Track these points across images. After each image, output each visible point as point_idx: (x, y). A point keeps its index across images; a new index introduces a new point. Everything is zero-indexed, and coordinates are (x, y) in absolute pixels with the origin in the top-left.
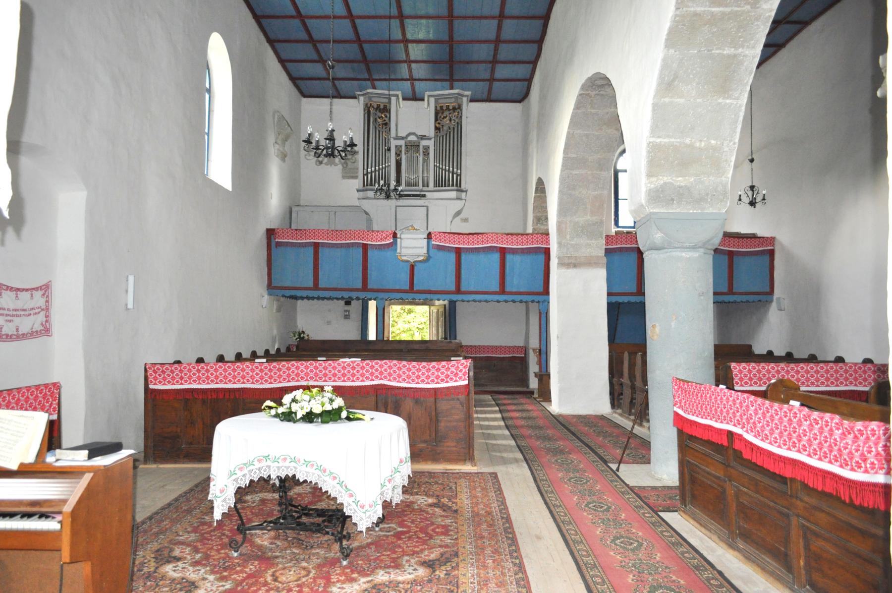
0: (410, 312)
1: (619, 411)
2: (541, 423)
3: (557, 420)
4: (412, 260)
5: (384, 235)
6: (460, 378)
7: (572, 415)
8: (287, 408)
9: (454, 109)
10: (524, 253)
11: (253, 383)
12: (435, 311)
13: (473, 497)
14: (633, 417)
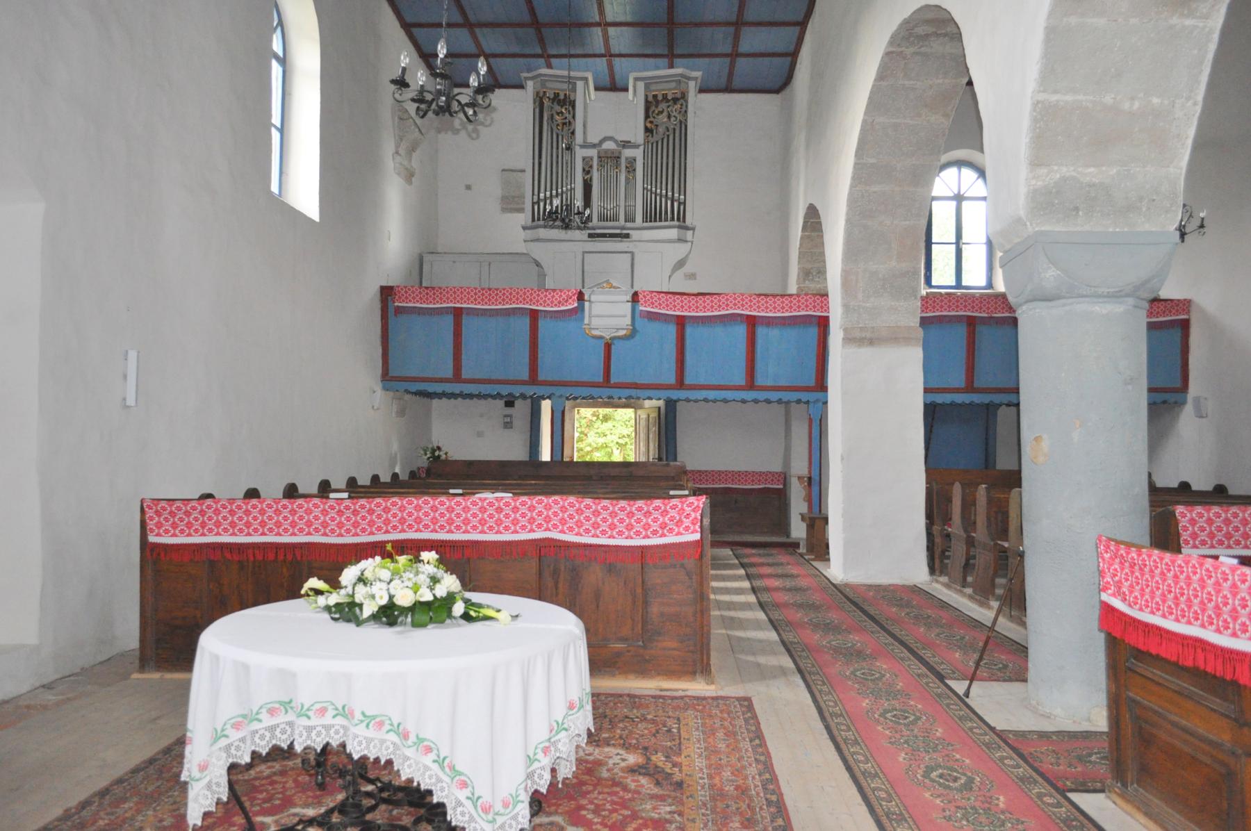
0: (606, 419)
1: (944, 579)
2: (816, 598)
3: (841, 592)
4: (607, 335)
5: (564, 296)
6: (687, 529)
7: (865, 585)
8: (348, 595)
9: (675, 100)
10: (784, 324)
11: (325, 534)
12: (644, 416)
13: (712, 751)
14: (969, 591)
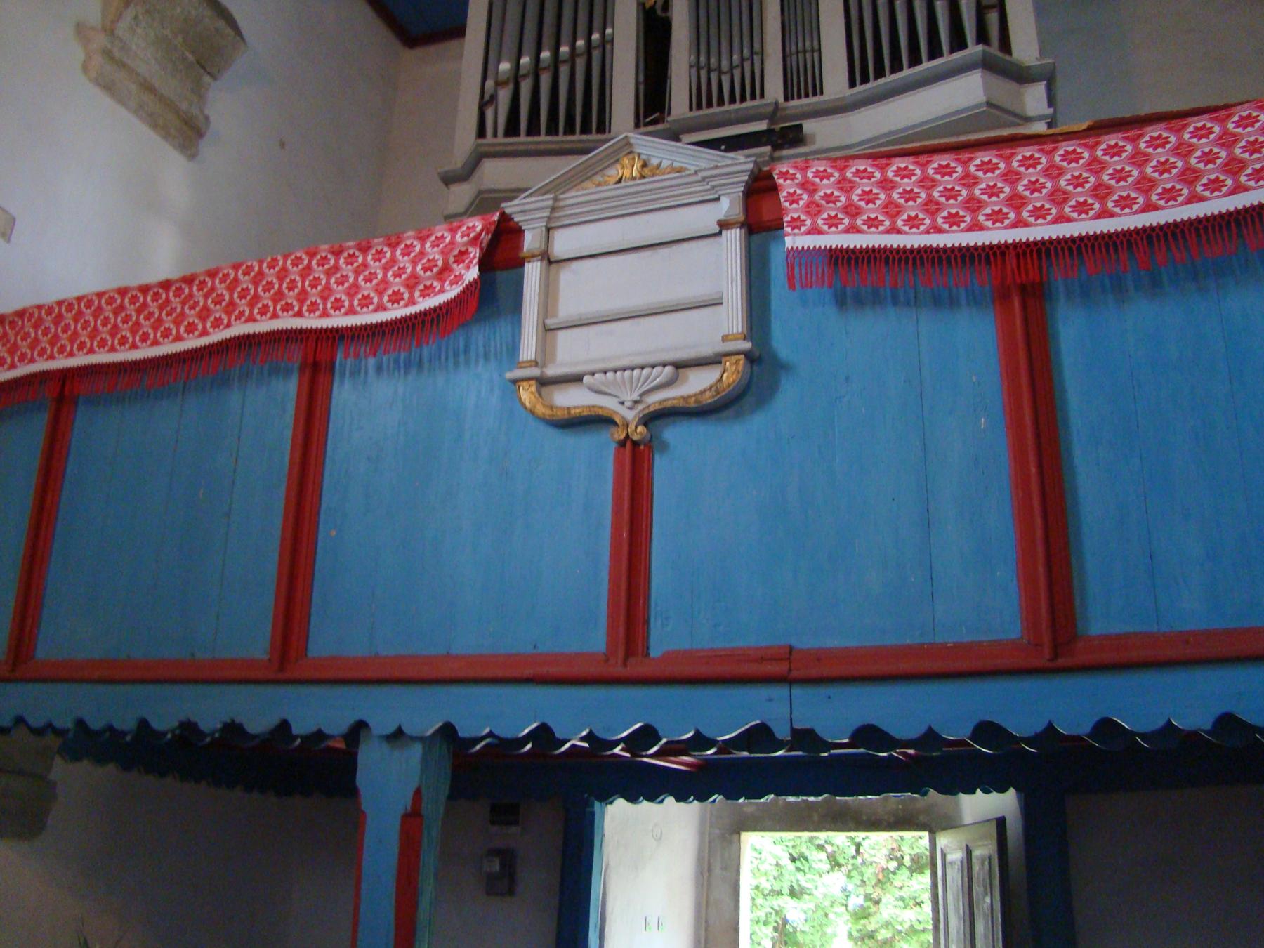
5: (434, 253)
